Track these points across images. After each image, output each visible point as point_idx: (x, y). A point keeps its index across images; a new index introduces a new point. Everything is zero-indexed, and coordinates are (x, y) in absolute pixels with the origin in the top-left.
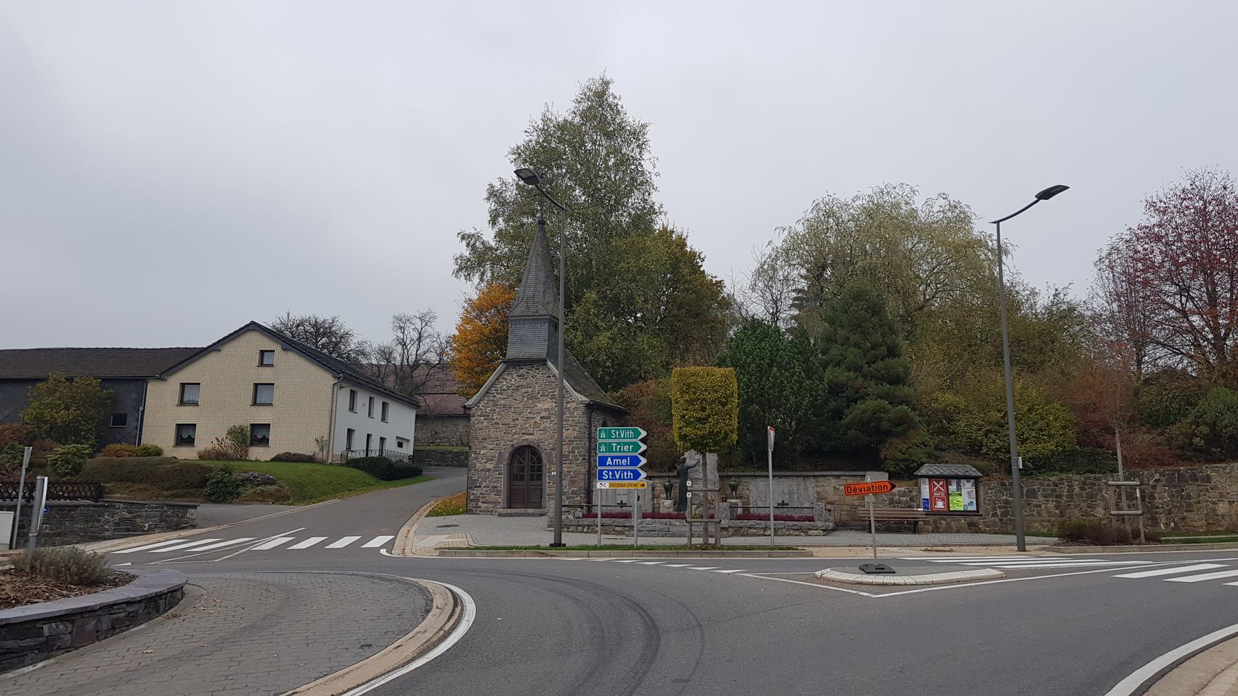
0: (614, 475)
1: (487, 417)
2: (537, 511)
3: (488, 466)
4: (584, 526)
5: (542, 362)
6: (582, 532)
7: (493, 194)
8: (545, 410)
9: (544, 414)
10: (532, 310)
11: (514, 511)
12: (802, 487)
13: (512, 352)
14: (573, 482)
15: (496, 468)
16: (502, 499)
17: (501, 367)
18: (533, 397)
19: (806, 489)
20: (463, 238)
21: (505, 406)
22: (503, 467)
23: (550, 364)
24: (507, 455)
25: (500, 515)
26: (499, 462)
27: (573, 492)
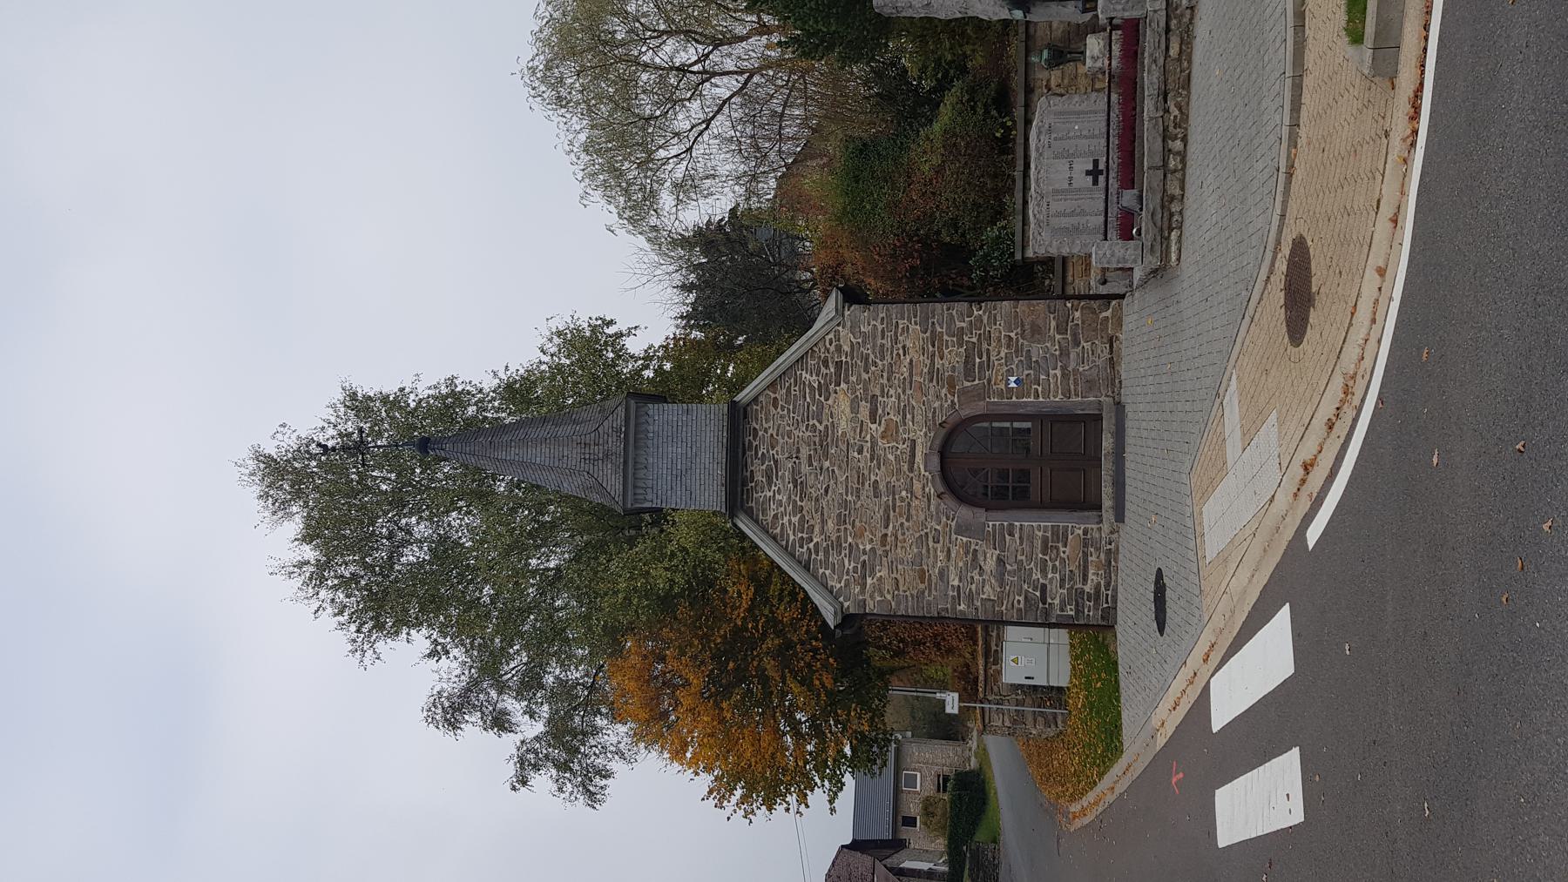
1: (866, 569)
2: (1107, 424)
3: (990, 564)
4: (1167, 151)
5: (738, 419)
6: (1183, 156)
8: (855, 409)
9: (865, 409)
13: (709, 495)
14: (1037, 331)
15: (997, 541)
16: (1076, 526)
17: (744, 525)
18: (823, 443)
20: (524, 783)
21: (841, 520)
23: (743, 396)
24: (965, 512)
25: (1120, 516)
27: (1061, 329)
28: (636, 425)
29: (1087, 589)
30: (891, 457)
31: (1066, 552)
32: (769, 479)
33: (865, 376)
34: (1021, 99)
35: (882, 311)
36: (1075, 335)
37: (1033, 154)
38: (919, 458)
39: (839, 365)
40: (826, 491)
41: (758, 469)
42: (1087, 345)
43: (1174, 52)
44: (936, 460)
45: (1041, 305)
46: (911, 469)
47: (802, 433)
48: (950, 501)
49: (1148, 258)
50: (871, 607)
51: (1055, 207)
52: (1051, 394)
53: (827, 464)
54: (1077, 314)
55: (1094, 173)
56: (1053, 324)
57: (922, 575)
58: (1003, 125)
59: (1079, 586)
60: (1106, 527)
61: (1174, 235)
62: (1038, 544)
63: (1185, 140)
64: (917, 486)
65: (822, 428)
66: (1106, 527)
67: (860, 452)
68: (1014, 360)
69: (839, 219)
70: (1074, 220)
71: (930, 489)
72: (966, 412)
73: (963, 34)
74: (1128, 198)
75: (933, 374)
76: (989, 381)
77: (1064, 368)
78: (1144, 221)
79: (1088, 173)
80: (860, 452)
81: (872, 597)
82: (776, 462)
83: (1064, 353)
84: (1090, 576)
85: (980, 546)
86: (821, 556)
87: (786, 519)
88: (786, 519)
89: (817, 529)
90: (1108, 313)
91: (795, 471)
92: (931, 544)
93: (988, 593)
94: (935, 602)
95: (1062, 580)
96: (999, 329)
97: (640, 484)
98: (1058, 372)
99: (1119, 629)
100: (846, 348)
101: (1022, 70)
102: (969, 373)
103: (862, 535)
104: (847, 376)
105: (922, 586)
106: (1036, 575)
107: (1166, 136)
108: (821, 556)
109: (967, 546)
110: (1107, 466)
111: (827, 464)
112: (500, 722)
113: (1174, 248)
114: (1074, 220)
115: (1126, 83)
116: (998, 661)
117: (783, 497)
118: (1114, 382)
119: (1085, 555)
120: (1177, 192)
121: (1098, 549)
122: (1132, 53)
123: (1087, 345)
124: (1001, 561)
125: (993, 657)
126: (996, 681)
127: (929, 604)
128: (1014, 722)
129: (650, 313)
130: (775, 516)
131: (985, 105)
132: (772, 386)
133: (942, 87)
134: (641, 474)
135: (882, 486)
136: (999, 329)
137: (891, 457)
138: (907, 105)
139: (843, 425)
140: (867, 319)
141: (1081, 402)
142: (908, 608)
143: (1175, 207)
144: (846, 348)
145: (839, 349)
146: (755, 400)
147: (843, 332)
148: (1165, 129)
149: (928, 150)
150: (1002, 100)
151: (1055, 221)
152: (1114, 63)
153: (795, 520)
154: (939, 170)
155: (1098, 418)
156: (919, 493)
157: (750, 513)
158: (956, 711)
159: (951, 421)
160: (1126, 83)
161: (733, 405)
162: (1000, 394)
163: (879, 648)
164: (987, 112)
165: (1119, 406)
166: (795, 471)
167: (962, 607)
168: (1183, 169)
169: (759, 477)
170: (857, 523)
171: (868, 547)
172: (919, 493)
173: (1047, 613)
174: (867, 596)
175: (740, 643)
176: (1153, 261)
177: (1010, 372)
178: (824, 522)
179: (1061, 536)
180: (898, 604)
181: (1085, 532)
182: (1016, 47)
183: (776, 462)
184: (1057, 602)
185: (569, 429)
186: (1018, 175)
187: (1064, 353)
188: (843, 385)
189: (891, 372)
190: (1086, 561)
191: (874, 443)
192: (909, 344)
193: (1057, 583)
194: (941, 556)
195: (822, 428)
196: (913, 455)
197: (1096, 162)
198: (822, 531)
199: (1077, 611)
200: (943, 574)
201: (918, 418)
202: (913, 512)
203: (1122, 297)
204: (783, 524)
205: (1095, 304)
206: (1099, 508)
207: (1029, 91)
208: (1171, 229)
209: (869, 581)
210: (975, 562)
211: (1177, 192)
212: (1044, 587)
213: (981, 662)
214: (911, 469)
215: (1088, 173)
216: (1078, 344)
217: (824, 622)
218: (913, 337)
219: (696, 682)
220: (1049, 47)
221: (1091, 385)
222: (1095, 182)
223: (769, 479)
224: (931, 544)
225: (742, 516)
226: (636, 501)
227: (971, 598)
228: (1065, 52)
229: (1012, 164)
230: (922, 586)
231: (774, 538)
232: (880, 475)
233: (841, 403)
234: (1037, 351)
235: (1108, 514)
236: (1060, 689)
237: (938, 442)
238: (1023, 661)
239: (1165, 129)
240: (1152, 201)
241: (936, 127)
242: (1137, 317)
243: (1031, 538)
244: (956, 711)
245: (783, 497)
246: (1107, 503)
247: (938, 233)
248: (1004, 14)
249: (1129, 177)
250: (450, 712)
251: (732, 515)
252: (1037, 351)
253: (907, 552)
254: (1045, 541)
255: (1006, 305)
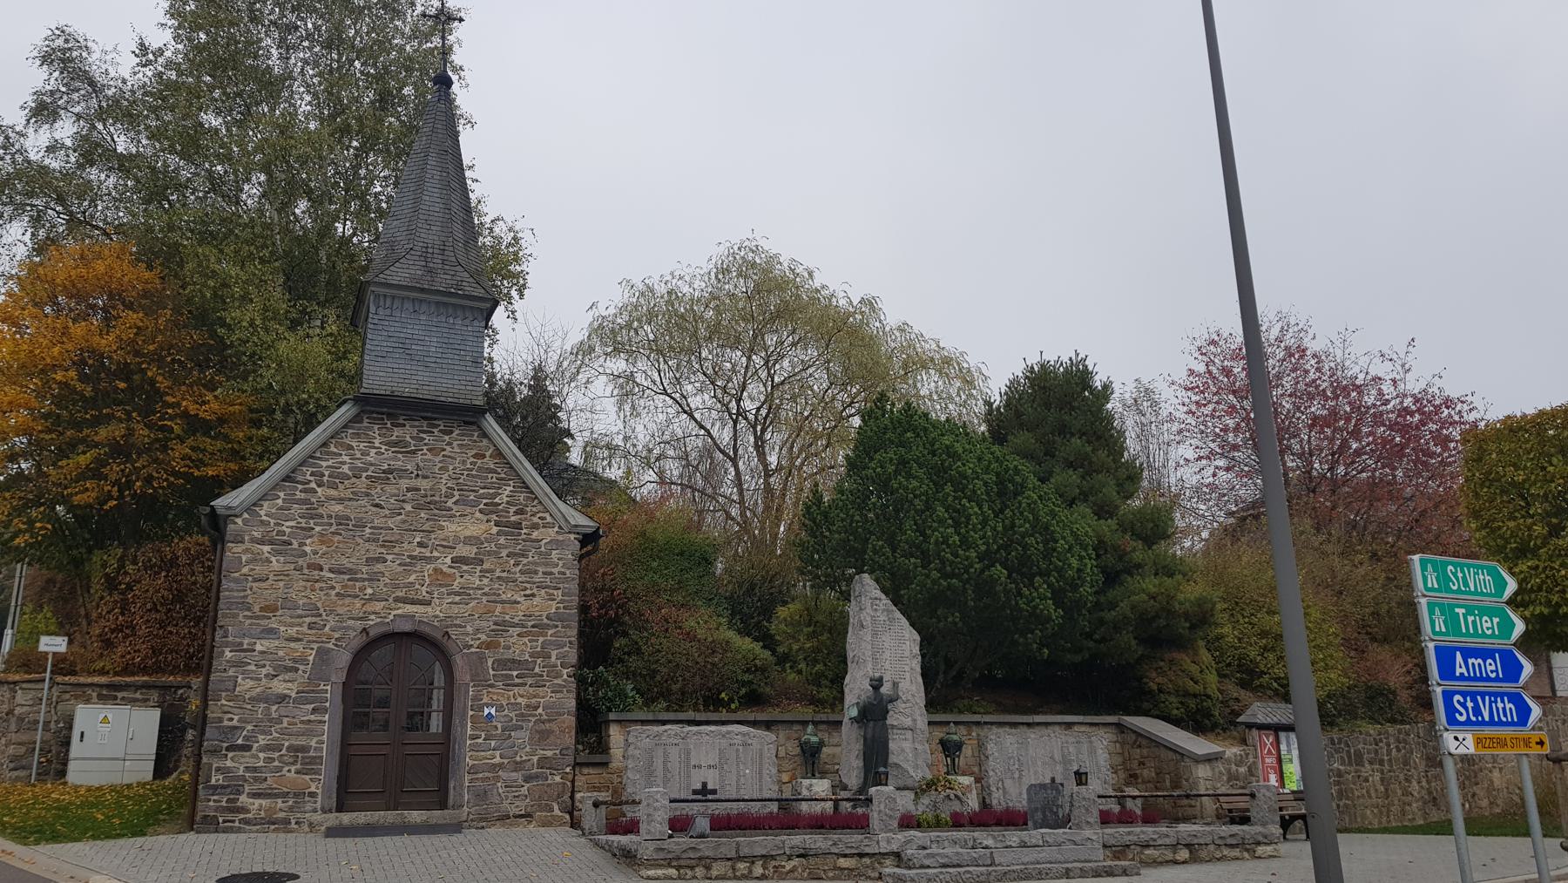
0: (1477, 711)
1: (281, 545)
2: (436, 816)
3: (279, 686)
4: (752, 859)
7: (64, 57)
8: (468, 541)
10: (443, 282)
11: (361, 818)
12: (1085, 747)
13: (380, 377)
14: (542, 736)
16: (321, 784)
17: (344, 412)
18: (433, 505)
19: (1092, 751)
21: (342, 520)
22: (330, 692)
23: (490, 423)
24: (344, 659)
25: (334, 832)
26: (319, 674)
27: (543, 762)
28: (463, 307)
29: (243, 798)
30: (412, 579)
31: (290, 773)
32: (396, 444)
33: (504, 553)
34: (761, 717)
35: (573, 573)
36: (537, 777)
37: (724, 729)
38: (410, 609)
39: (518, 526)
40: (377, 506)
41: (406, 433)
42: (524, 791)
43: (842, 862)
44: (407, 627)
45: (569, 739)
46: (397, 600)
47: (445, 482)
48: (357, 642)
49: (651, 846)
50: (233, 550)
51: (674, 753)
52: (475, 753)
53: (408, 507)
54: (558, 779)
55: (704, 792)
56: (549, 753)
57: (270, 609)
58: (731, 700)
59: (247, 789)
60: (317, 817)
61: (672, 872)
62: (301, 741)
63: (763, 877)
64: (379, 606)
65: (449, 504)
66: (317, 817)
67: (420, 545)
68: (511, 713)
69: (643, 534)
70: (660, 772)
71: (373, 620)
72: (458, 661)
73: (816, 661)
74: (703, 824)
75: (503, 626)
76: (492, 686)
77: (501, 766)
78: (682, 841)
79: (705, 784)
80: (420, 545)
81: (247, 551)
82: (414, 452)
83: (518, 766)
84: (257, 802)
85: (302, 676)
86: (300, 495)
87: (346, 459)
88: (346, 459)
89: (333, 492)
90: (557, 812)
91: (402, 473)
92: (308, 620)
93: (245, 685)
94: (234, 626)
95: (255, 769)
96: (547, 696)
97: (397, 303)
98: (498, 760)
99: (192, 836)
100: (535, 534)
101: (787, 717)
102: (501, 664)
103: (322, 543)
104: (506, 534)
105: (256, 608)
106: (262, 740)
107: (766, 858)
108: (300, 495)
109: (304, 661)
110: (390, 816)
111: (408, 507)
112: (44, 111)
113: (660, 872)
114: (660, 772)
115: (786, 818)
116: (102, 698)
117: (372, 457)
118: (484, 820)
119: (285, 795)
120: (714, 873)
121: (291, 809)
122: (818, 824)
123: (524, 791)
124: (282, 698)
125: (109, 694)
126: (76, 697)
127: (235, 616)
128: (21, 719)
129: (515, 344)
130: (351, 448)
131: (751, 682)
132: (499, 454)
133: (768, 641)
134: (408, 305)
135: (380, 567)
136: (547, 696)
137: (412, 579)
138: (752, 606)
139: (451, 528)
140: (564, 560)
141: (463, 786)
142: (229, 591)
143: (700, 871)
144: (535, 534)
145: (535, 527)
146: (485, 435)
147: (552, 532)
148: (773, 857)
149: (710, 626)
150: (754, 699)
151: (660, 752)
152: (804, 807)
153: (345, 469)
154: (690, 636)
155: (443, 805)
156: (368, 608)
157: (356, 419)
158: (42, 648)
159: (450, 645)
160: (786, 818)
161: (479, 412)
162: (476, 698)
163: (122, 560)
164: (744, 684)
165: (456, 828)
166: (402, 473)
167: (228, 654)
168: (736, 878)
169: (397, 432)
170: (337, 538)
171: (308, 549)
172: (368, 608)
173: (215, 752)
174: (248, 545)
175: (148, 399)
176: (647, 851)
177: (500, 708)
178: (341, 500)
179: (310, 766)
180: (236, 581)
181: (312, 795)
182: (805, 712)
183: (414, 452)
184: (229, 763)
185: (459, 235)
186: (691, 715)
187: (518, 766)
188: (495, 530)
189: (507, 581)
190: (276, 796)
191: (429, 560)
192: (536, 601)
193: (252, 762)
194: (292, 631)
195: (449, 504)
196: (413, 603)
197: (714, 792)
198: (329, 499)
199: (215, 787)
200: (270, 632)
201: (455, 609)
202: (348, 600)
203: (575, 824)
204: (341, 453)
205: (566, 797)
206: (340, 809)
207: (768, 725)
208: (678, 868)
209: (266, 548)
210: (281, 669)
211: (714, 873)
212: (247, 748)
213: (103, 680)
214: (397, 600)
215: (705, 784)
216: (527, 779)
217: (219, 496)
218: (544, 605)
219: (106, 343)
220: (821, 744)
221: (481, 796)
222: (695, 792)
223: (396, 444)
224: (308, 620)
225: (354, 411)
226: (377, 296)
227: (239, 664)
228: (811, 760)
229: (696, 710)
230: (256, 608)
231: (325, 444)
232: (392, 566)
233: (476, 526)
234: (521, 737)
235: (333, 819)
236: (62, 773)
237: (427, 630)
238: (105, 728)
239: (773, 857)
240: (706, 847)
241: (731, 634)
242: (560, 838)
243: (308, 734)
244: (42, 648)
245: (372, 457)
246: (346, 818)
247: (625, 634)
248: (850, 699)
249: (722, 824)
250: (64, 57)
251: (356, 400)
252: (521, 737)
253: (299, 592)
254: (305, 749)
255: (572, 703)
